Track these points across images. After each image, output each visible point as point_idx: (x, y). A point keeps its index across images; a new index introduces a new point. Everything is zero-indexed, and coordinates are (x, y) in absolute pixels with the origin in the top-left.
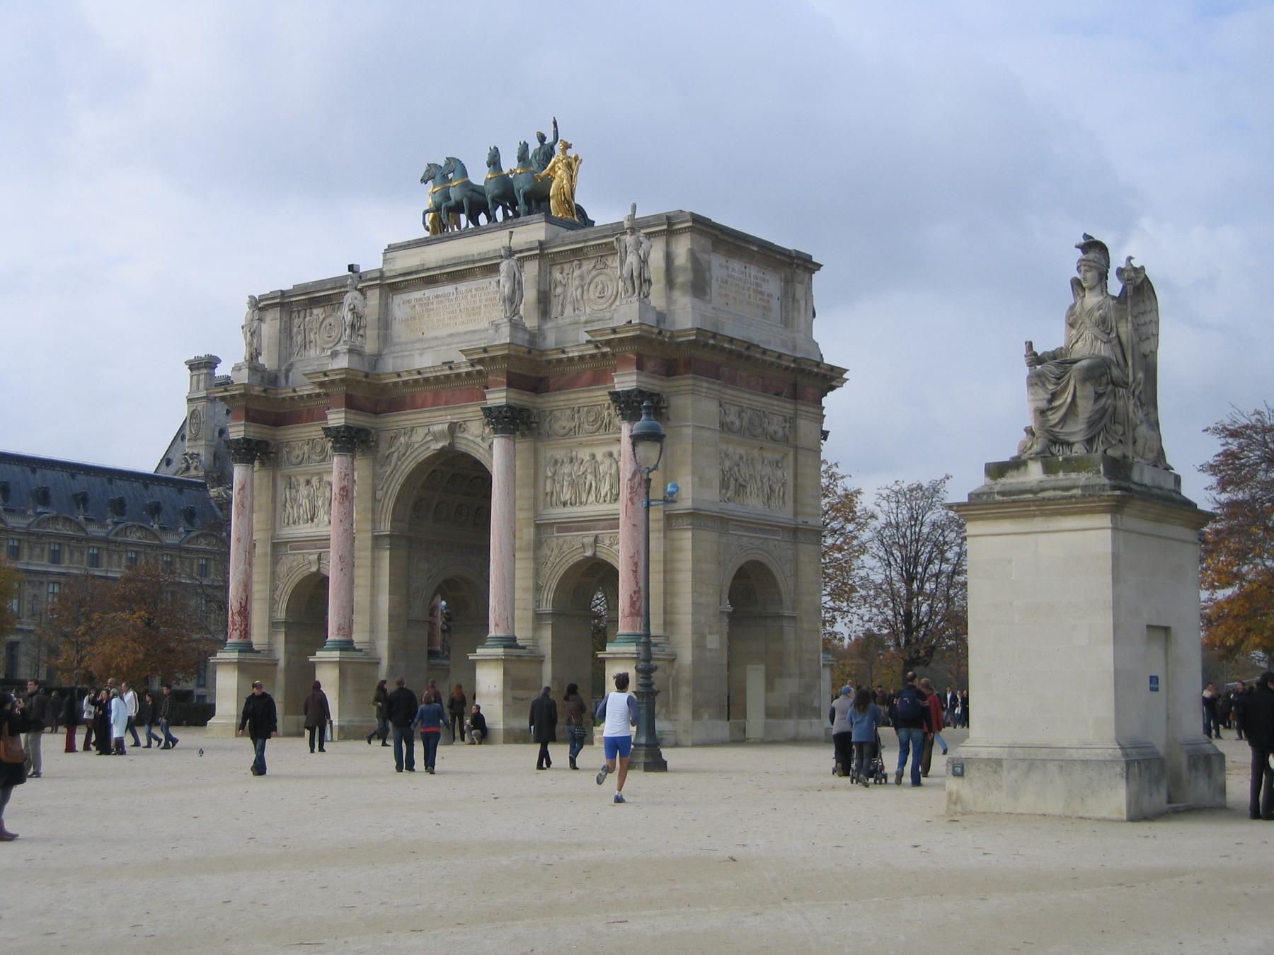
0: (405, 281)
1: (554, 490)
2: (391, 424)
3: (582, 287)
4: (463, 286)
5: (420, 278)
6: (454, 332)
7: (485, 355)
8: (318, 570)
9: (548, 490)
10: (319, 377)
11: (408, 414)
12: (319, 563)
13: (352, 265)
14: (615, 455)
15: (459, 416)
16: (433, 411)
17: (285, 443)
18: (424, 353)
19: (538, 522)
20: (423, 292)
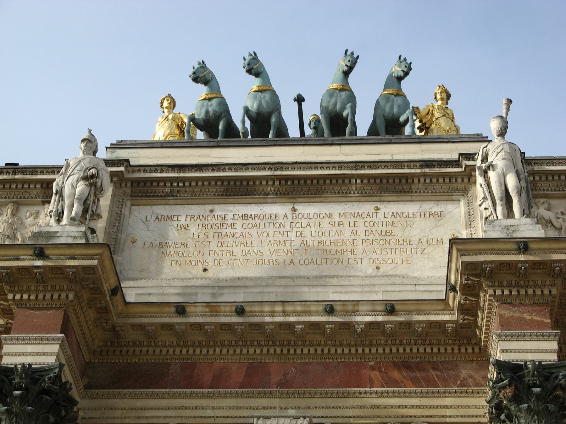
0: (178, 180)
2: (118, 413)
5: (217, 179)
6: (284, 274)
7: (522, 257)
10: (18, 259)
15: (321, 412)
20: (209, 207)
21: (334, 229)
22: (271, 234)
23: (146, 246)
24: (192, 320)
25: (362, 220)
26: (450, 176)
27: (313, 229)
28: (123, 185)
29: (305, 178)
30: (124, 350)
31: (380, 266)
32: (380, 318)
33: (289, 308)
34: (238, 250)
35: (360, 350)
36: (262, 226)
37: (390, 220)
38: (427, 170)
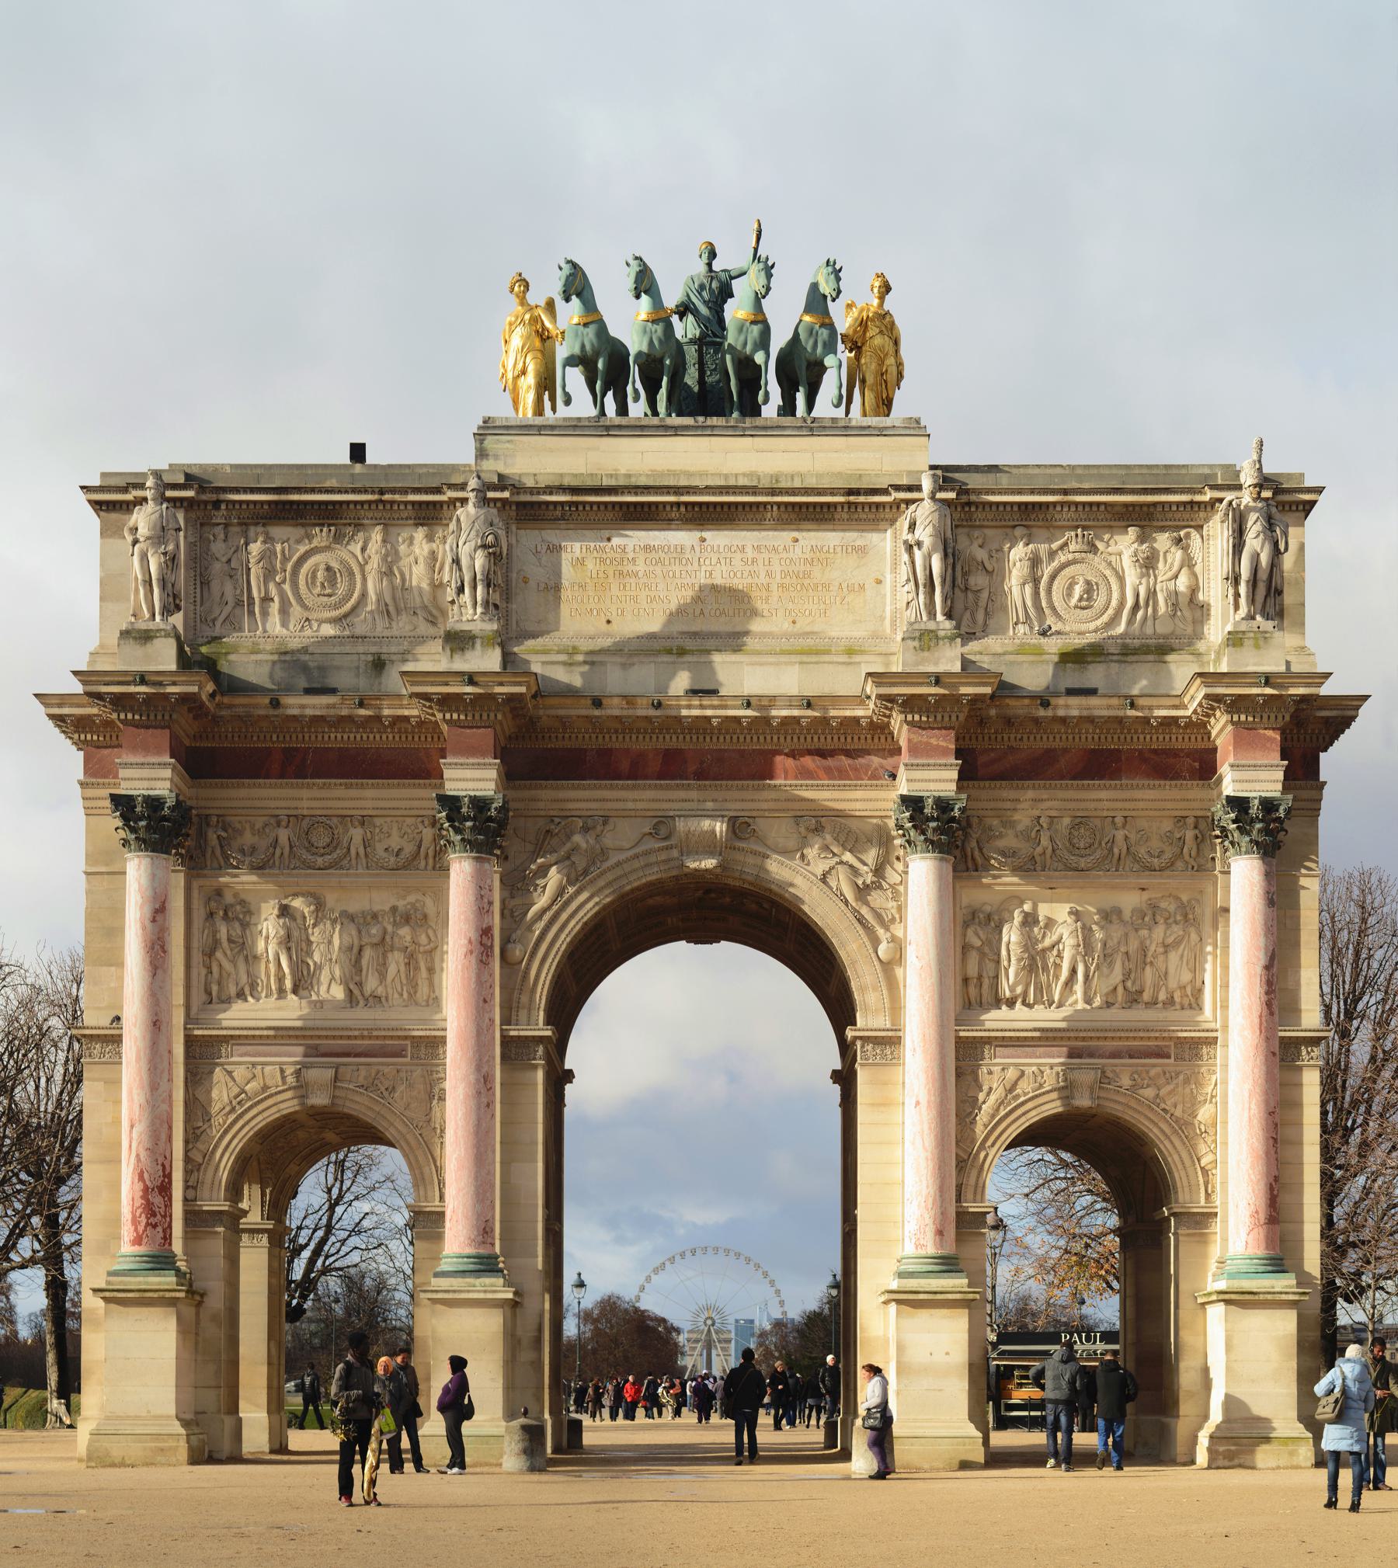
0: (571, 504)
1: (984, 974)
2: (541, 805)
3: (1036, 582)
4: (719, 538)
5: (614, 504)
6: (694, 629)
8: (333, 1104)
9: (972, 970)
11: (595, 787)
12: (335, 1087)
13: (363, 446)
14: (1127, 915)
15: (739, 805)
16: (668, 788)
17: (215, 819)
18: (634, 664)
19: (962, 1034)
21: (748, 568)
22: (678, 574)
23: (541, 588)
24: (609, 712)
25: (777, 556)
26: (878, 505)
27: (724, 568)
28: (507, 507)
29: (715, 504)
30: (540, 736)
31: (797, 619)
32: (796, 713)
33: (706, 702)
34: (643, 594)
35: (775, 738)
36: (667, 563)
37: (808, 556)
38: (852, 498)
